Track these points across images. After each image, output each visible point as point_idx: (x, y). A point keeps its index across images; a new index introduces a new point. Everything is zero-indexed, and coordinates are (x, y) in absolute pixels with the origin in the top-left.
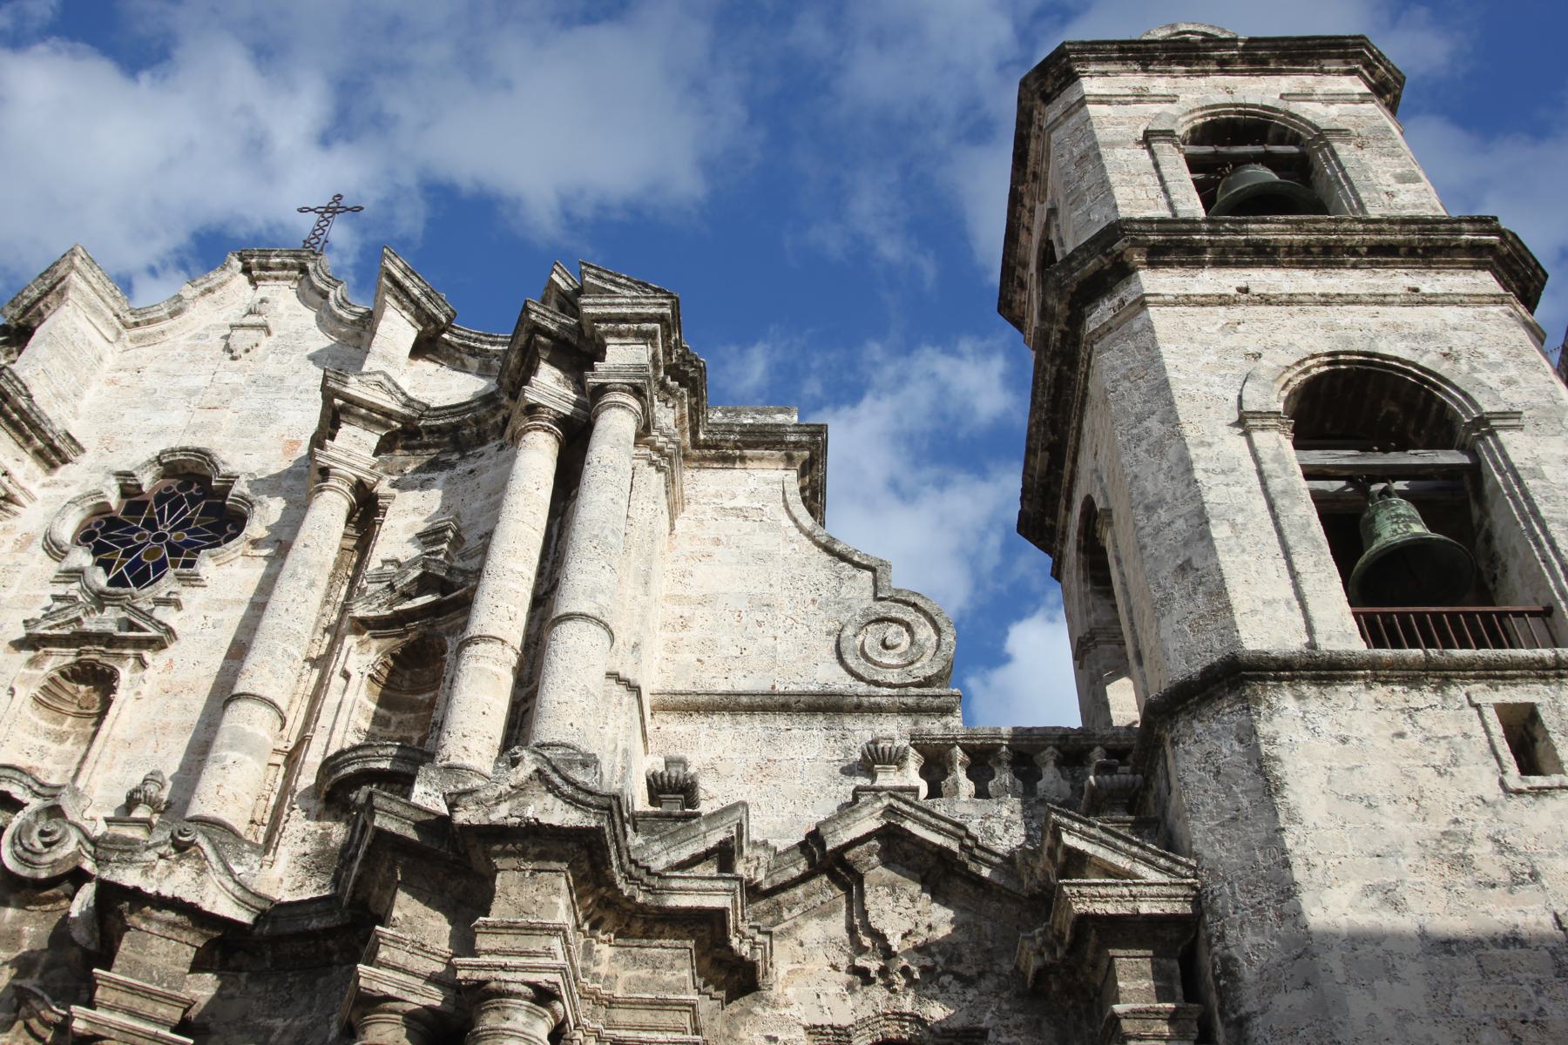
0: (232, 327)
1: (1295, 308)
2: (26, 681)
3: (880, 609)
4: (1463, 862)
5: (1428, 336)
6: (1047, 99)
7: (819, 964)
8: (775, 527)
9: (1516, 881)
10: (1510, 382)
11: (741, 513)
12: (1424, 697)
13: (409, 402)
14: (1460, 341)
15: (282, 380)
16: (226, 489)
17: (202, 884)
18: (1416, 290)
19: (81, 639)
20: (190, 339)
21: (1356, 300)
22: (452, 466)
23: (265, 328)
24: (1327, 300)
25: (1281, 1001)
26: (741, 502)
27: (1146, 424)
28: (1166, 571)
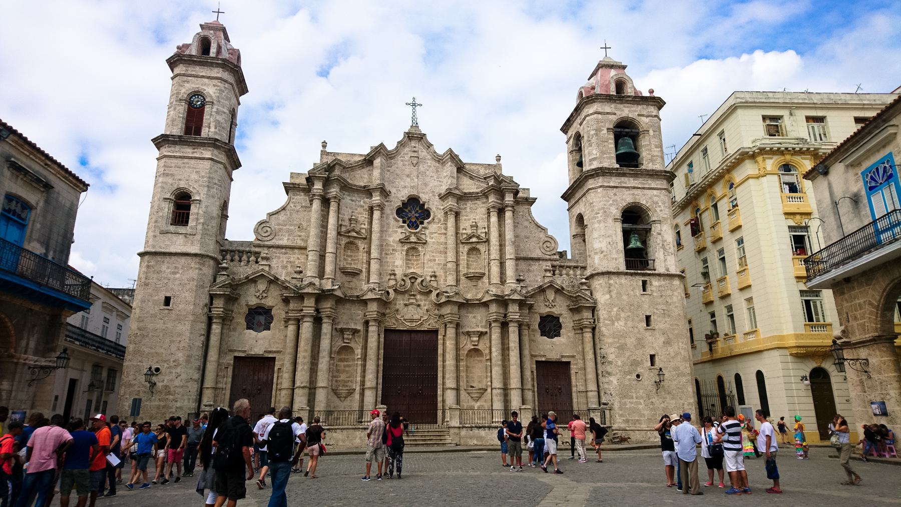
0: (411, 157)
2: (402, 250)
3: (546, 239)
8: (527, 220)
10: (661, 211)
13: (462, 192)
14: (656, 199)
16: (424, 205)
19: (411, 242)
21: (639, 188)
24: (634, 188)
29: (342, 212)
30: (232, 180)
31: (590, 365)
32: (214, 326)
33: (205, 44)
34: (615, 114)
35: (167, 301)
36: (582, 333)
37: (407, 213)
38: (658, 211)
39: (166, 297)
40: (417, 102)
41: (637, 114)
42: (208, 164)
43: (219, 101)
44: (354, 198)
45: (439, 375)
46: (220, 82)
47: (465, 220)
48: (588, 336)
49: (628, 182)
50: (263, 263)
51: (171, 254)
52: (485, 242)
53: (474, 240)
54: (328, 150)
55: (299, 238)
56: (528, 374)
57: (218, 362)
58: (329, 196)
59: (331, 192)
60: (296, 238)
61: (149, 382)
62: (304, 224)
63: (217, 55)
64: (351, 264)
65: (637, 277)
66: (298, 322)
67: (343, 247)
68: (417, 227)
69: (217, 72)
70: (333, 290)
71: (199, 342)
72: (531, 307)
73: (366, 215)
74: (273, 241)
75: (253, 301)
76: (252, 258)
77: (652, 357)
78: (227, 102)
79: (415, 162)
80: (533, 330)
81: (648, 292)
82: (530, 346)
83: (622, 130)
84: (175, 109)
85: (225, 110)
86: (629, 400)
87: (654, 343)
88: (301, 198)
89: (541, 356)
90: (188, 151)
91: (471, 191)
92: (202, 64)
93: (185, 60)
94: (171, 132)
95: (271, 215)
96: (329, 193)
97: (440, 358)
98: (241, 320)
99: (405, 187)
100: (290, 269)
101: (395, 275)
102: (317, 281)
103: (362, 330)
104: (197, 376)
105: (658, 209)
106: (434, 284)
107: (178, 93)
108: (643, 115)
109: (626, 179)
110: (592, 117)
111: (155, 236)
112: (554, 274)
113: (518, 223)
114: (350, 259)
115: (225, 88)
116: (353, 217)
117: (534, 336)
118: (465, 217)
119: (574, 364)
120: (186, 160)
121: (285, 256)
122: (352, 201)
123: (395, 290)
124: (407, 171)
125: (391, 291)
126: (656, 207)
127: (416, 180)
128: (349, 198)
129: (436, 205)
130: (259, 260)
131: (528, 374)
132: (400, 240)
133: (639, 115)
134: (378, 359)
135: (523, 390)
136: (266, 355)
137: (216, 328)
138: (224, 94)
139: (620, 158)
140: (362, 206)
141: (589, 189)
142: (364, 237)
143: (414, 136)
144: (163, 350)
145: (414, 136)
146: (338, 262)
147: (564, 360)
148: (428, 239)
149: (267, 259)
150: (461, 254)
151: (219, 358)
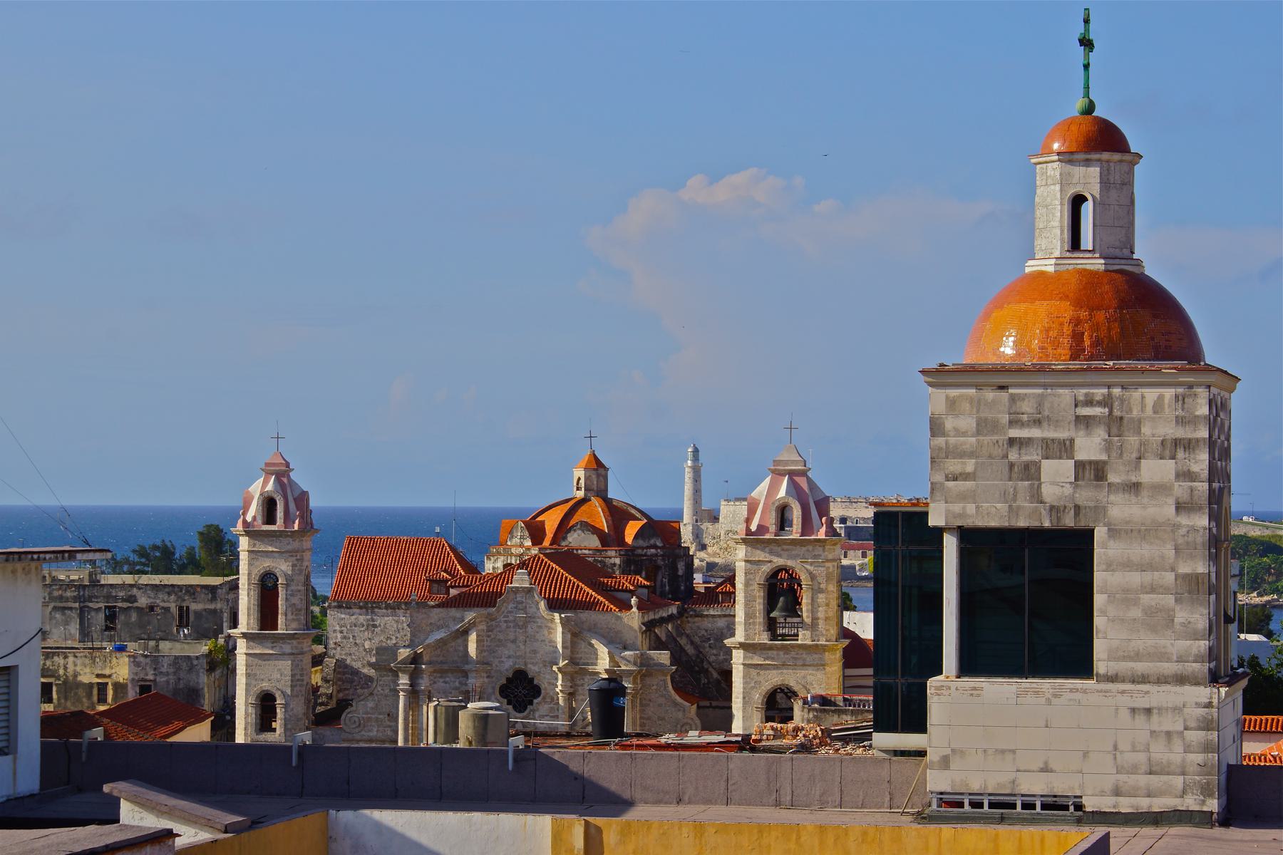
3: (685, 721)
8: (662, 696)
44: (448, 679)
55: (389, 729)
60: (386, 729)
85: (300, 588)
99: (509, 657)
107: (249, 574)
113: (650, 700)
122: (446, 682)
124: (511, 636)
127: (522, 647)
128: (441, 680)
129: (548, 679)
138: (296, 568)
140: (456, 689)
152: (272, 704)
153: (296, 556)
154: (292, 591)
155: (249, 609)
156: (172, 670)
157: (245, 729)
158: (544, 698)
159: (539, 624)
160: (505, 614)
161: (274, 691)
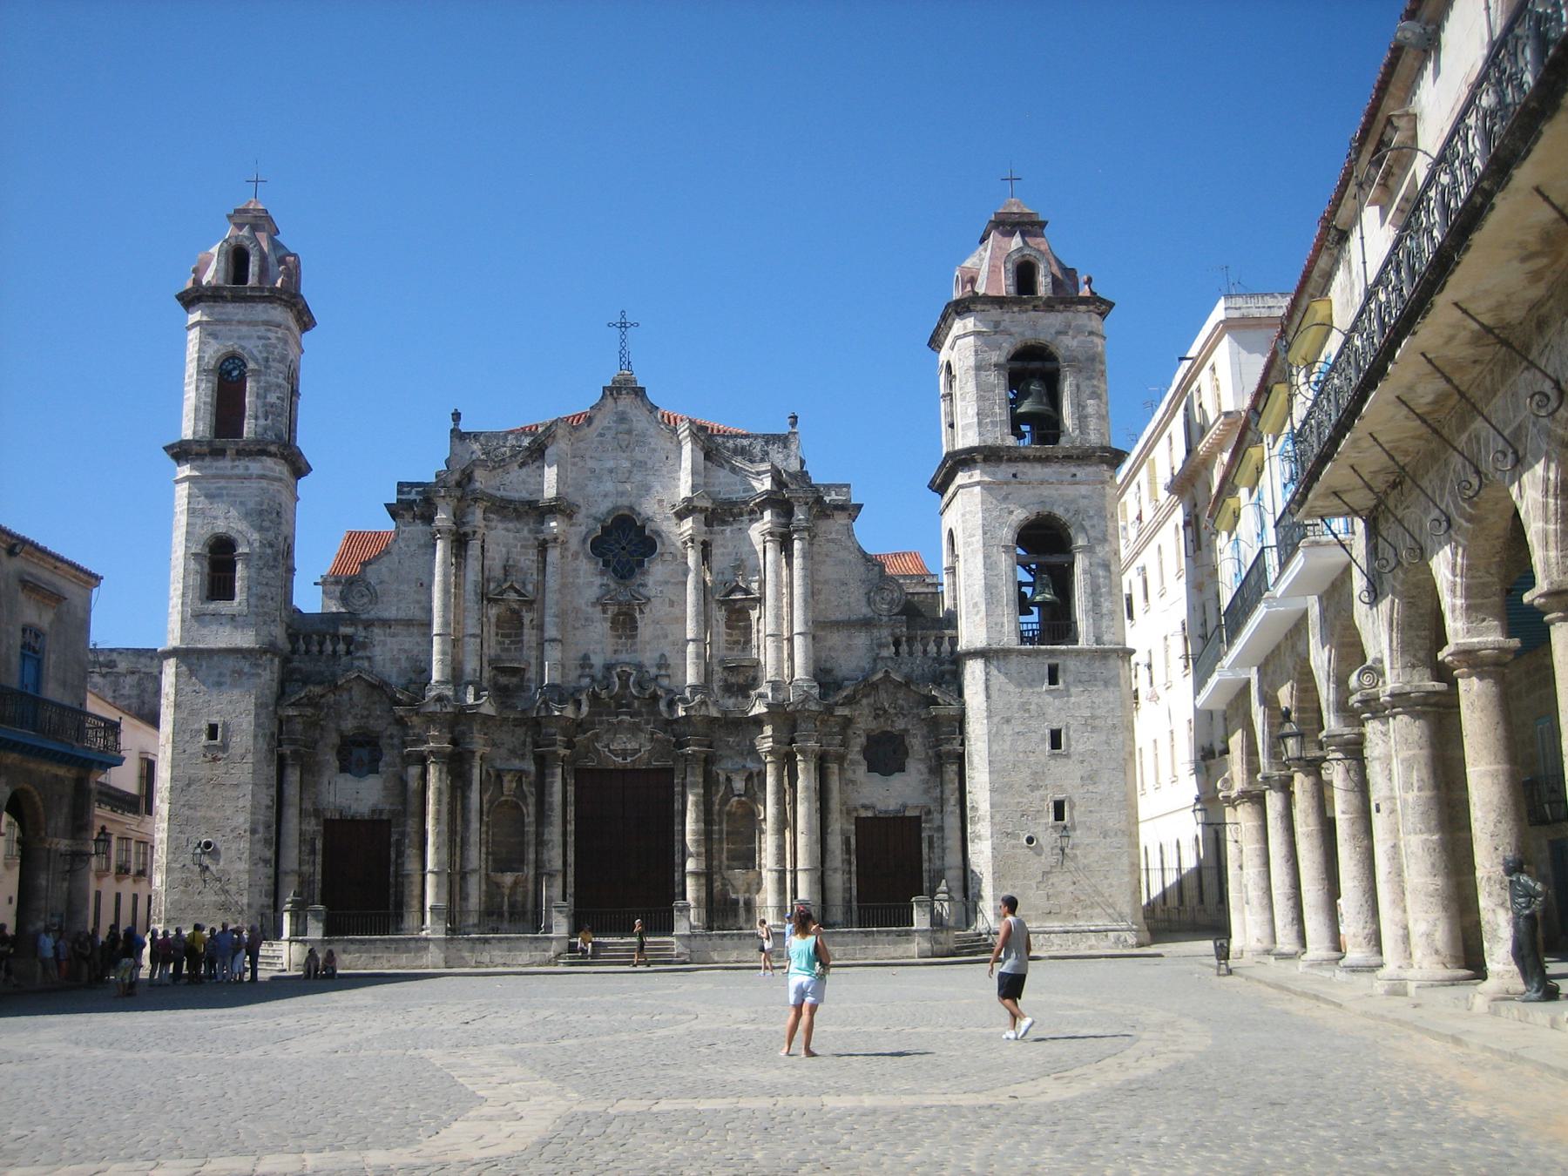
1: (1030, 486)
2: (605, 619)
4: (1028, 711)
5: (1073, 501)
6: (959, 314)
7: (866, 711)
8: (846, 548)
9: (1039, 716)
11: (833, 541)
12: (1029, 660)
14: (1083, 503)
15: (646, 463)
17: (708, 709)
18: (1074, 475)
19: (620, 604)
20: (598, 436)
22: (731, 524)
23: (629, 432)
24: (1042, 483)
25: (979, 744)
26: (834, 536)
27: (973, 539)
28: (971, 603)
29: (488, 554)
30: (297, 499)
31: (952, 822)
32: (289, 771)
33: (238, 259)
34: (1010, 334)
35: (213, 731)
36: (941, 765)
37: (611, 545)
38: (1088, 527)
39: (210, 725)
40: (629, 319)
41: (1053, 331)
42: (254, 484)
43: (268, 367)
45: (676, 848)
46: (269, 330)
47: (723, 554)
48: (952, 769)
49: (1030, 472)
50: (358, 655)
51: (211, 652)
52: (760, 599)
53: (739, 596)
54: (464, 427)
55: (417, 606)
56: (835, 842)
57: (301, 829)
58: (468, 529)
59: (468, 523)
61: (200, 865)
62: (425, 580)
63: (260, 281)
64: (508, 650)
65: (1040, 658)
66: (422, 760)
67: (493, 620)
68: (631, 573)
69: (261, 311)
70: (478, 705)
71: (267, 796)
72: (848, 722)
73: (532, 555)
74: (373, 613)
75: (349, 725)
76: (341, 647)
77: (1059, 808)
78: (281, 367)
79: (624, 444)
80: (853, 763)
81: (1061, 685)
82: (841, 791)
83: (1026, 364)
84: (197, 388)
85: (280, 381)
86: (1010, 883)
87: (1065, 777)
88: (419, 528)
89: (865, 807)
90: (225, 464)
91: (734, 497)
92: (238, 298)
93: (207, 296)
94: (194, 433)
95: (365, 564)
96: (464, 523)
97: (677, 820)
98: (331, 759)
100: (404, 664)
101: (591, 666)
102: (449, 692)
103: (533, 768)
104: (270, 854)
105: (1087, 524)
106: (665, 682)
107: (200, 359)
108: (1066, 333)
109: (1028, 465)
110: (966, 339)
111: (183, 621)
112: (897, 653)
114: (507, 641)
115: (278, 338)
116: (511, 562)
117: (854, 772)
118: (722, 550)
119: (926, 822)
120: (222, 483)
121: (394, 640)
122: (507, 530)
123: (594, 698)
125: (584, 698)
126: (1083, 520)
128: (500, 526)
130: (352, 648)
131: (835, 842)
132: (598, 599)
133: (1059, 333)
134: (565, 822)
135: (823, 873)
136: (376, 817)
137: (293, 776)
139: (1016, 422)
141: (960, 487)
142: (531, 598)
143: (624, 389)
144: (213, 814)
145: (624, 389)
146: (485, 650)
147: (907, 814)
148: (652, 593)
149: (363, 646)
150: (714, 622)
151: (300, 823)
152: (227, 557)
153: (276, 333)
154: (267, 382)
155: (197, 409)
156: (135, 692)
157: (184, 595)
158: (662, 555)
159: (652, 446)
160: (600, 430)
161: (233, 534)
